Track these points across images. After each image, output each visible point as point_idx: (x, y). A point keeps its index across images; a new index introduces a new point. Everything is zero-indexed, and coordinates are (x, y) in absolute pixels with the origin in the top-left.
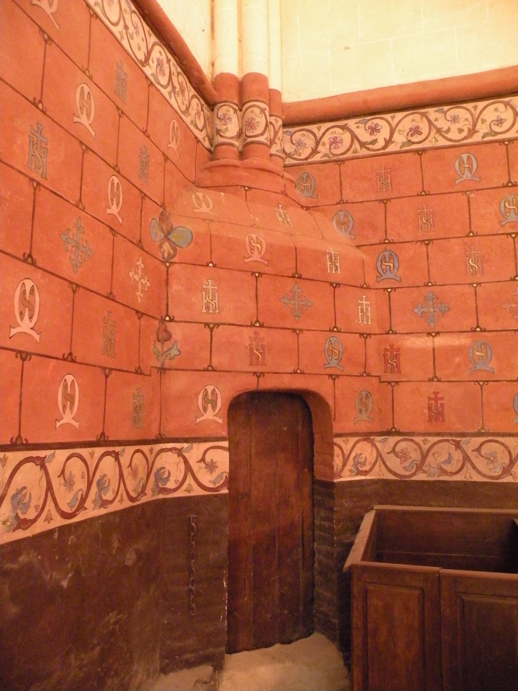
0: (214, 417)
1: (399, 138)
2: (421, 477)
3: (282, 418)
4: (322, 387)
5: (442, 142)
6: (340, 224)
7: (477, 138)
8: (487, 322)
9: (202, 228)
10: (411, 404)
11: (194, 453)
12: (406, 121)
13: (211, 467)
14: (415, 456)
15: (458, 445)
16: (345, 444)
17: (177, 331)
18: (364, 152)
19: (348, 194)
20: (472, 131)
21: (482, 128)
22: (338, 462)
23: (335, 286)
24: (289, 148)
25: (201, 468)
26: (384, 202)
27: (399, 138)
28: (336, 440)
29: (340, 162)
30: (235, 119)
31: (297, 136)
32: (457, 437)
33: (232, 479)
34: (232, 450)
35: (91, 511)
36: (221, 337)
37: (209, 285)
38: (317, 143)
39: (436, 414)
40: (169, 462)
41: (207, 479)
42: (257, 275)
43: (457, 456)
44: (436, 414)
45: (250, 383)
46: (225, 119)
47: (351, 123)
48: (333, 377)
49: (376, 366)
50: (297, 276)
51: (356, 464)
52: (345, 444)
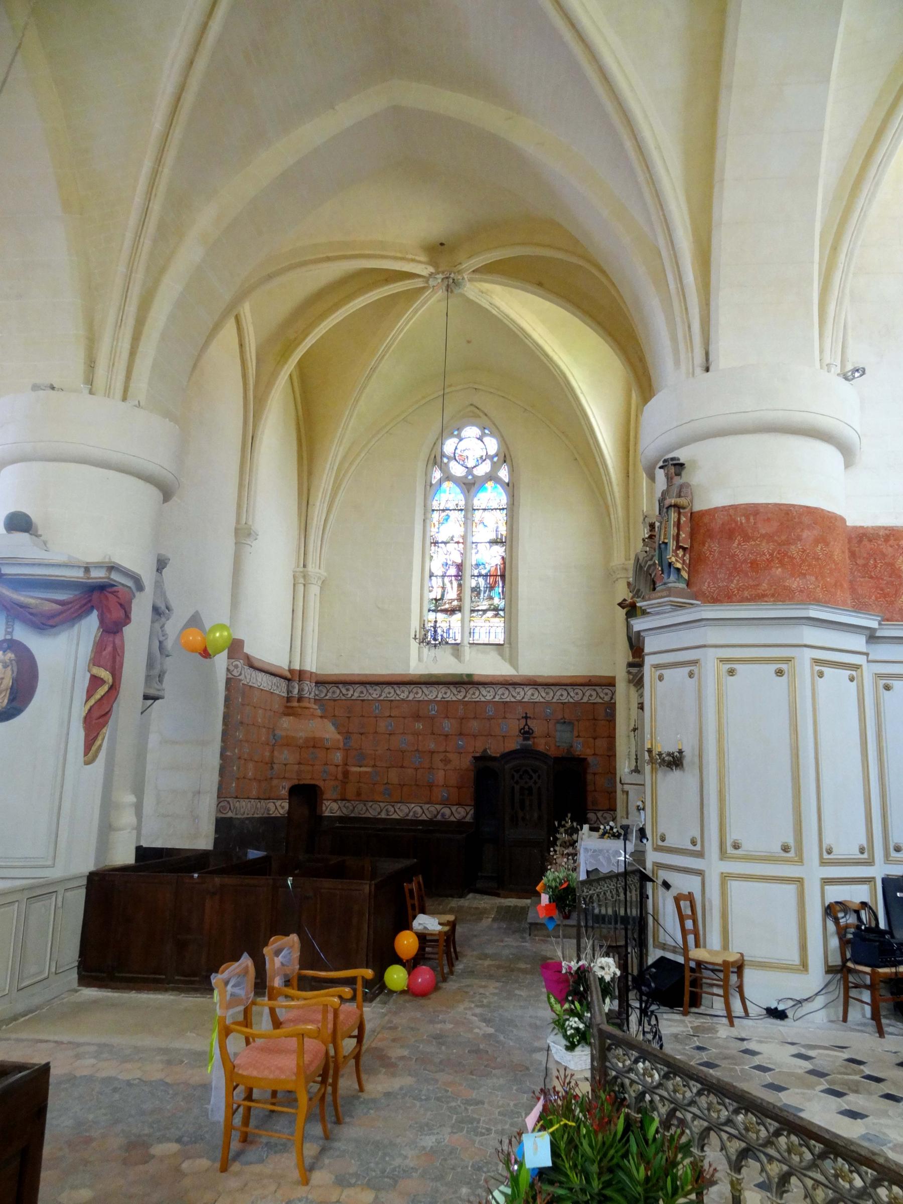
0: (284, 792)
1: (356, 695)
2: (353, 815)
3: (305, 795)
4: (321, 784)
5: (370, 698)
6: (333, 724)
7: (382, 698)
8: (378, 763)
9: (284, 734)
10: (351, 790)
11: (278, 803)
12: (360, 688)
13: (283, 808)
14: (351, 808)
15: (365, 805)
16: (327, 803)
17: (275, 766)
18: (343, 698)
19: (337, 713)
20: (380, 696)
21: (384, 695)
22: (324, 808)
23: (327, 749)
24: (317, 693)
25: (280, 808)
26: (349, 717)
27: (356, 695)
28: (325, 802)
29: (335, 700)
30: (297, 686)
31: (320, 688)
32: (365, 802)
33: (289, 812)
34: (290, 803)
35: (256, 816)
36: (289, 767)
37: (286, 752)
38: (328, 691)
39: (359, 794)
40: (271, 806)
41: (282, 811)
42: (301, 748)
43: (364, 808)
44: (359, 794)
45: (296, 782)
46: (293, 687)
47: (340, 686)
48: (324, 780)
49: (340, 776)
50: (314, 747)
51: (331, 810)
52: (327, 803)
